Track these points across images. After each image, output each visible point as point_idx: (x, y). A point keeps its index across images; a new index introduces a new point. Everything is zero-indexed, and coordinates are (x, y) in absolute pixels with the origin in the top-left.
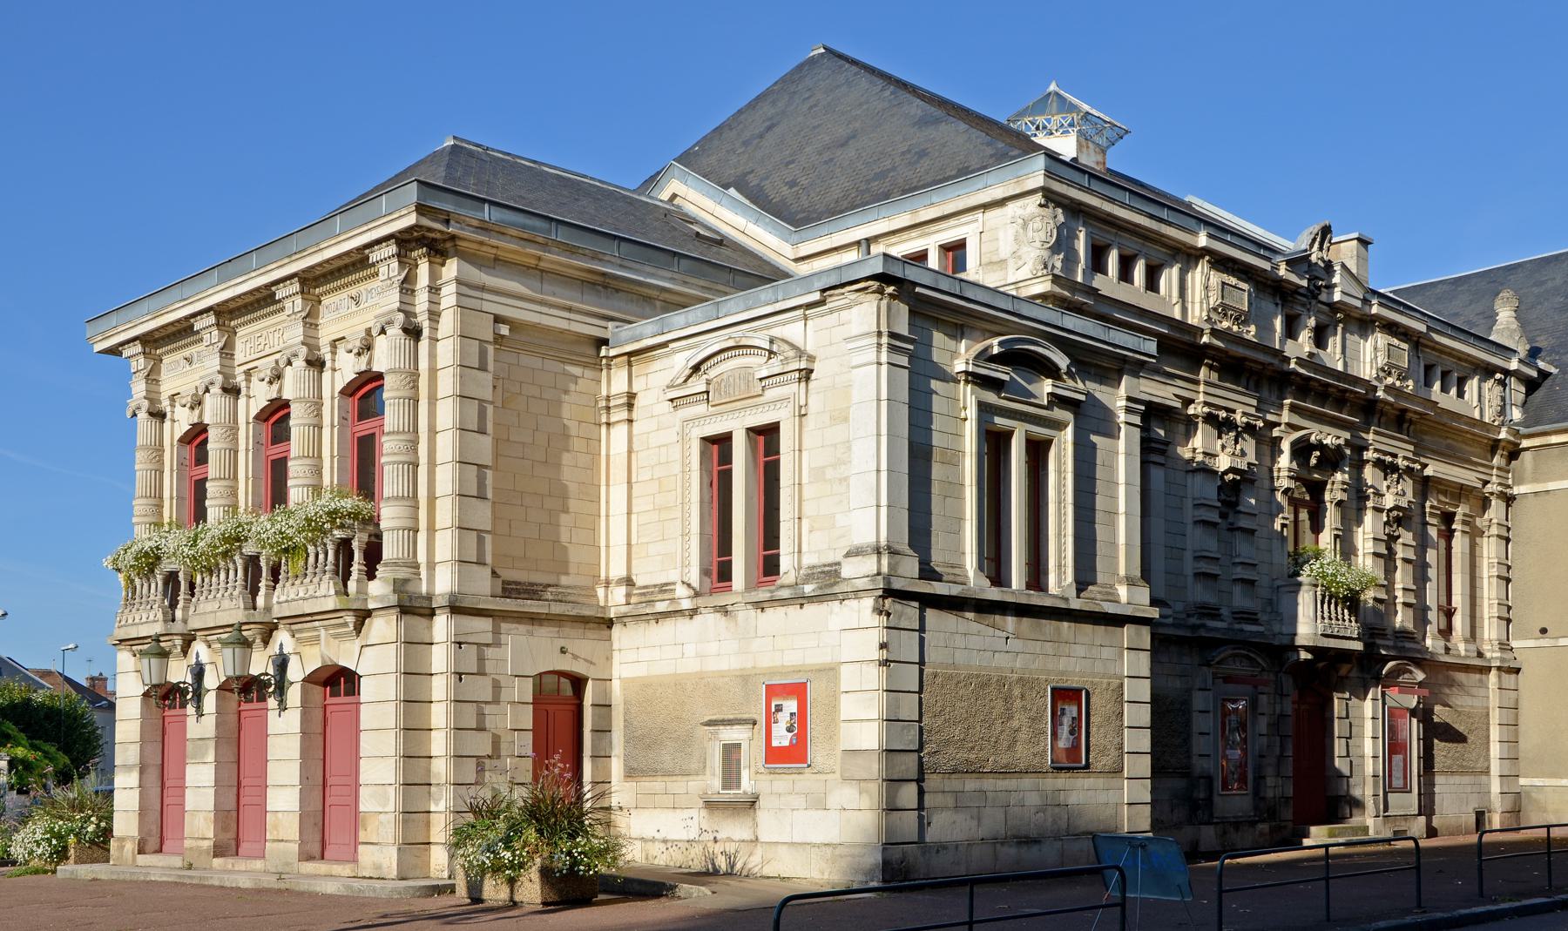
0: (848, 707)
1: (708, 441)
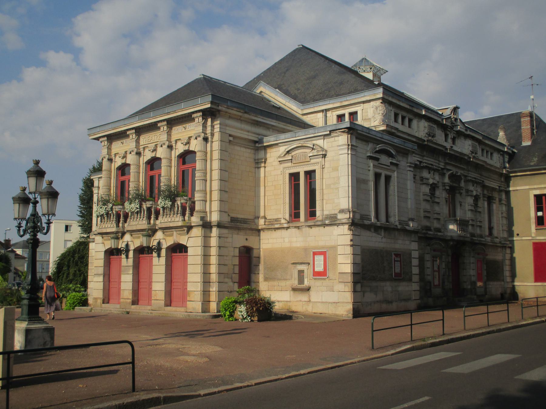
0: (340, 259)
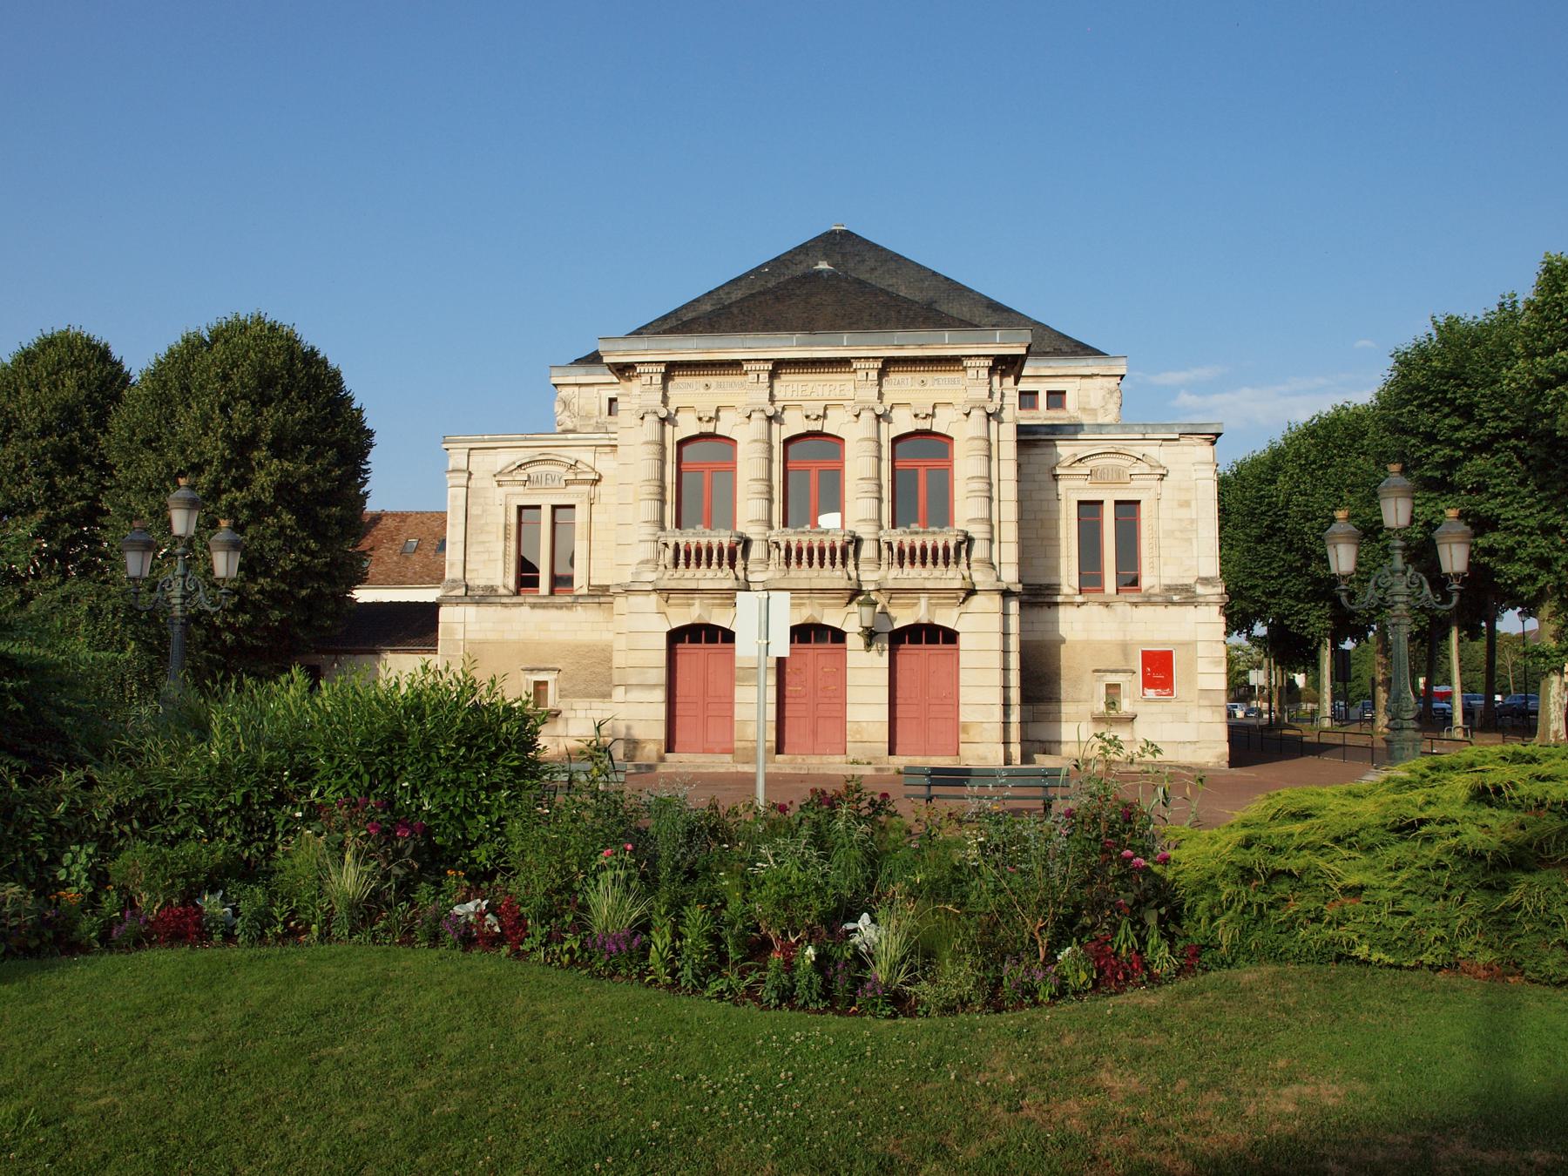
0: (1202, 666)
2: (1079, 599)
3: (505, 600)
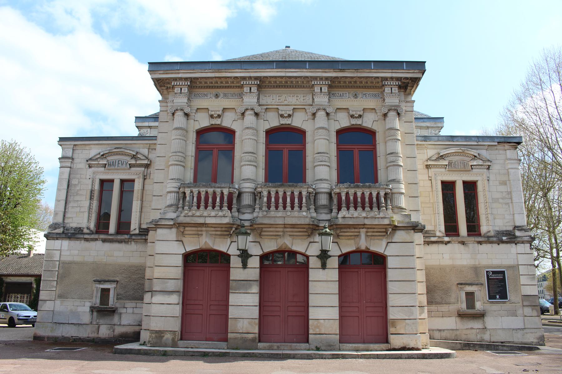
1: (102, 182)
2: (447, 239)
3: (86, 236)
